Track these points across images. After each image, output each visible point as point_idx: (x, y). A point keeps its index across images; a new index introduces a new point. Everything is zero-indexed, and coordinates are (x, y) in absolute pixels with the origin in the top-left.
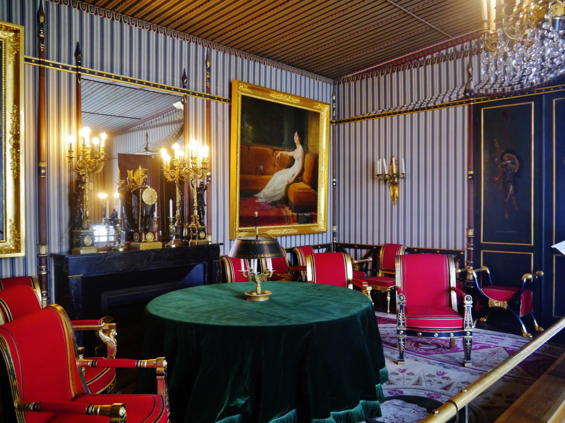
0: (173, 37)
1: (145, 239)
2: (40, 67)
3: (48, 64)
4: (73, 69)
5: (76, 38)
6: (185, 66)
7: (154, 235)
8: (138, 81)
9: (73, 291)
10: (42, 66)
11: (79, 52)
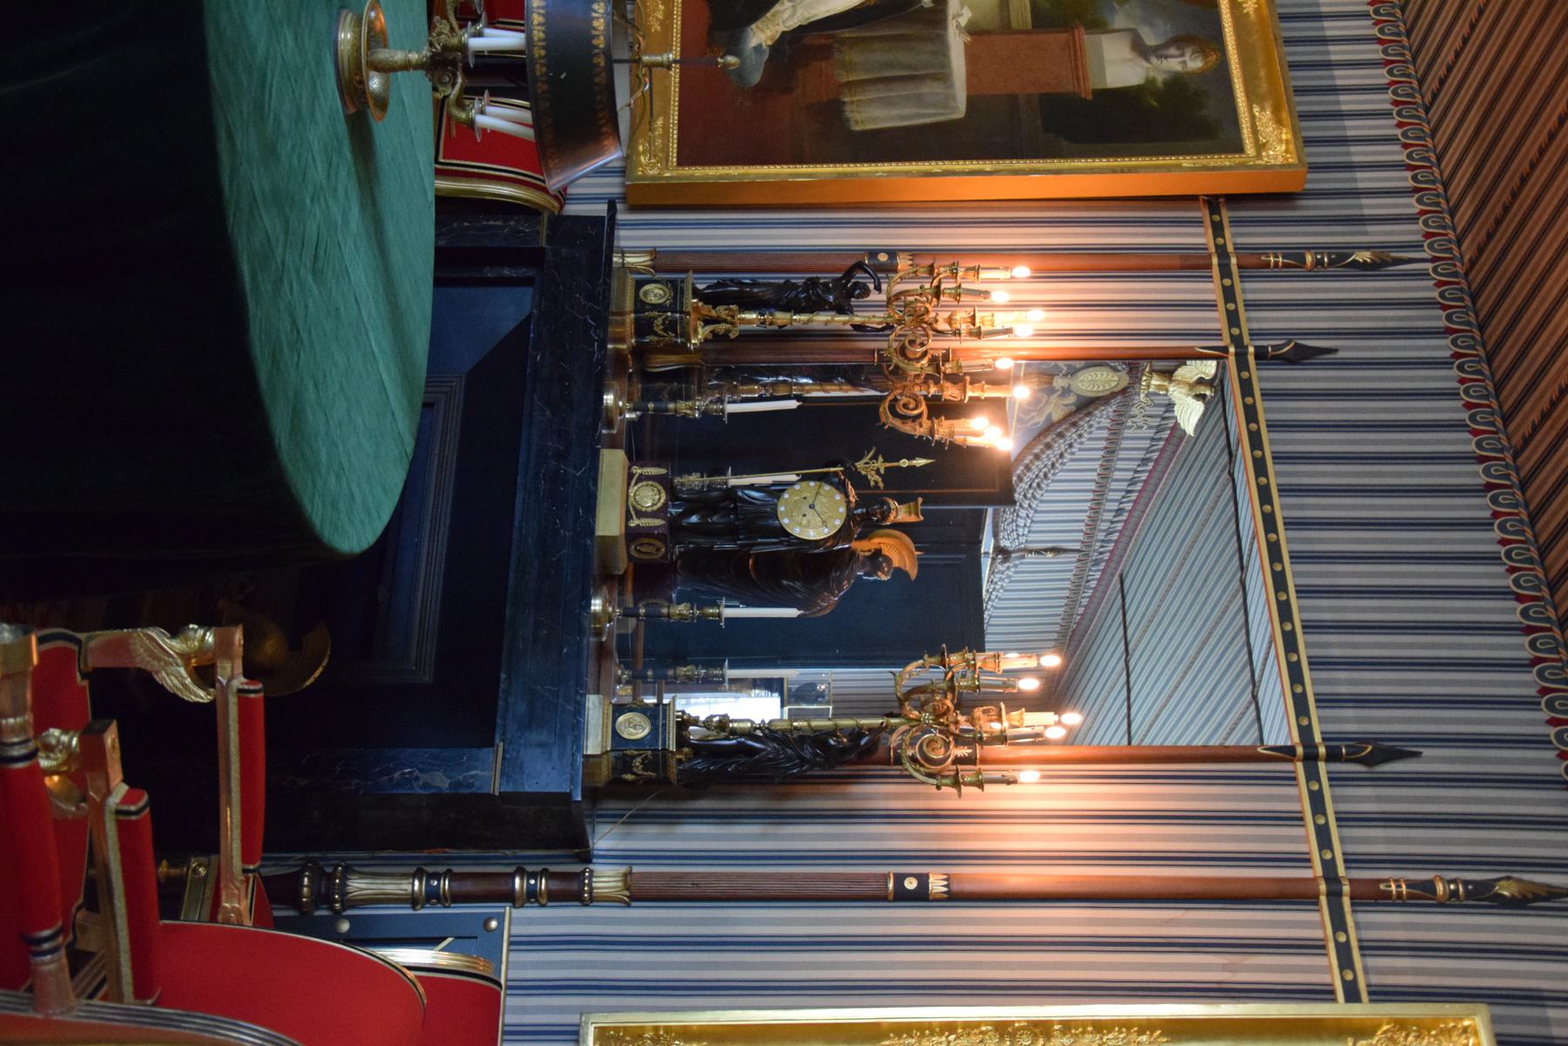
0: (1543, 701)
1: (641, 478)
2: (1210, 256)
3: (1225, 271)
4: (1237, 340)
5: (1349, 349)
6: (1433, 760)
7: (654, 515)
9: (499, 223)
10: (1215, 260)
11: (1300, 356)
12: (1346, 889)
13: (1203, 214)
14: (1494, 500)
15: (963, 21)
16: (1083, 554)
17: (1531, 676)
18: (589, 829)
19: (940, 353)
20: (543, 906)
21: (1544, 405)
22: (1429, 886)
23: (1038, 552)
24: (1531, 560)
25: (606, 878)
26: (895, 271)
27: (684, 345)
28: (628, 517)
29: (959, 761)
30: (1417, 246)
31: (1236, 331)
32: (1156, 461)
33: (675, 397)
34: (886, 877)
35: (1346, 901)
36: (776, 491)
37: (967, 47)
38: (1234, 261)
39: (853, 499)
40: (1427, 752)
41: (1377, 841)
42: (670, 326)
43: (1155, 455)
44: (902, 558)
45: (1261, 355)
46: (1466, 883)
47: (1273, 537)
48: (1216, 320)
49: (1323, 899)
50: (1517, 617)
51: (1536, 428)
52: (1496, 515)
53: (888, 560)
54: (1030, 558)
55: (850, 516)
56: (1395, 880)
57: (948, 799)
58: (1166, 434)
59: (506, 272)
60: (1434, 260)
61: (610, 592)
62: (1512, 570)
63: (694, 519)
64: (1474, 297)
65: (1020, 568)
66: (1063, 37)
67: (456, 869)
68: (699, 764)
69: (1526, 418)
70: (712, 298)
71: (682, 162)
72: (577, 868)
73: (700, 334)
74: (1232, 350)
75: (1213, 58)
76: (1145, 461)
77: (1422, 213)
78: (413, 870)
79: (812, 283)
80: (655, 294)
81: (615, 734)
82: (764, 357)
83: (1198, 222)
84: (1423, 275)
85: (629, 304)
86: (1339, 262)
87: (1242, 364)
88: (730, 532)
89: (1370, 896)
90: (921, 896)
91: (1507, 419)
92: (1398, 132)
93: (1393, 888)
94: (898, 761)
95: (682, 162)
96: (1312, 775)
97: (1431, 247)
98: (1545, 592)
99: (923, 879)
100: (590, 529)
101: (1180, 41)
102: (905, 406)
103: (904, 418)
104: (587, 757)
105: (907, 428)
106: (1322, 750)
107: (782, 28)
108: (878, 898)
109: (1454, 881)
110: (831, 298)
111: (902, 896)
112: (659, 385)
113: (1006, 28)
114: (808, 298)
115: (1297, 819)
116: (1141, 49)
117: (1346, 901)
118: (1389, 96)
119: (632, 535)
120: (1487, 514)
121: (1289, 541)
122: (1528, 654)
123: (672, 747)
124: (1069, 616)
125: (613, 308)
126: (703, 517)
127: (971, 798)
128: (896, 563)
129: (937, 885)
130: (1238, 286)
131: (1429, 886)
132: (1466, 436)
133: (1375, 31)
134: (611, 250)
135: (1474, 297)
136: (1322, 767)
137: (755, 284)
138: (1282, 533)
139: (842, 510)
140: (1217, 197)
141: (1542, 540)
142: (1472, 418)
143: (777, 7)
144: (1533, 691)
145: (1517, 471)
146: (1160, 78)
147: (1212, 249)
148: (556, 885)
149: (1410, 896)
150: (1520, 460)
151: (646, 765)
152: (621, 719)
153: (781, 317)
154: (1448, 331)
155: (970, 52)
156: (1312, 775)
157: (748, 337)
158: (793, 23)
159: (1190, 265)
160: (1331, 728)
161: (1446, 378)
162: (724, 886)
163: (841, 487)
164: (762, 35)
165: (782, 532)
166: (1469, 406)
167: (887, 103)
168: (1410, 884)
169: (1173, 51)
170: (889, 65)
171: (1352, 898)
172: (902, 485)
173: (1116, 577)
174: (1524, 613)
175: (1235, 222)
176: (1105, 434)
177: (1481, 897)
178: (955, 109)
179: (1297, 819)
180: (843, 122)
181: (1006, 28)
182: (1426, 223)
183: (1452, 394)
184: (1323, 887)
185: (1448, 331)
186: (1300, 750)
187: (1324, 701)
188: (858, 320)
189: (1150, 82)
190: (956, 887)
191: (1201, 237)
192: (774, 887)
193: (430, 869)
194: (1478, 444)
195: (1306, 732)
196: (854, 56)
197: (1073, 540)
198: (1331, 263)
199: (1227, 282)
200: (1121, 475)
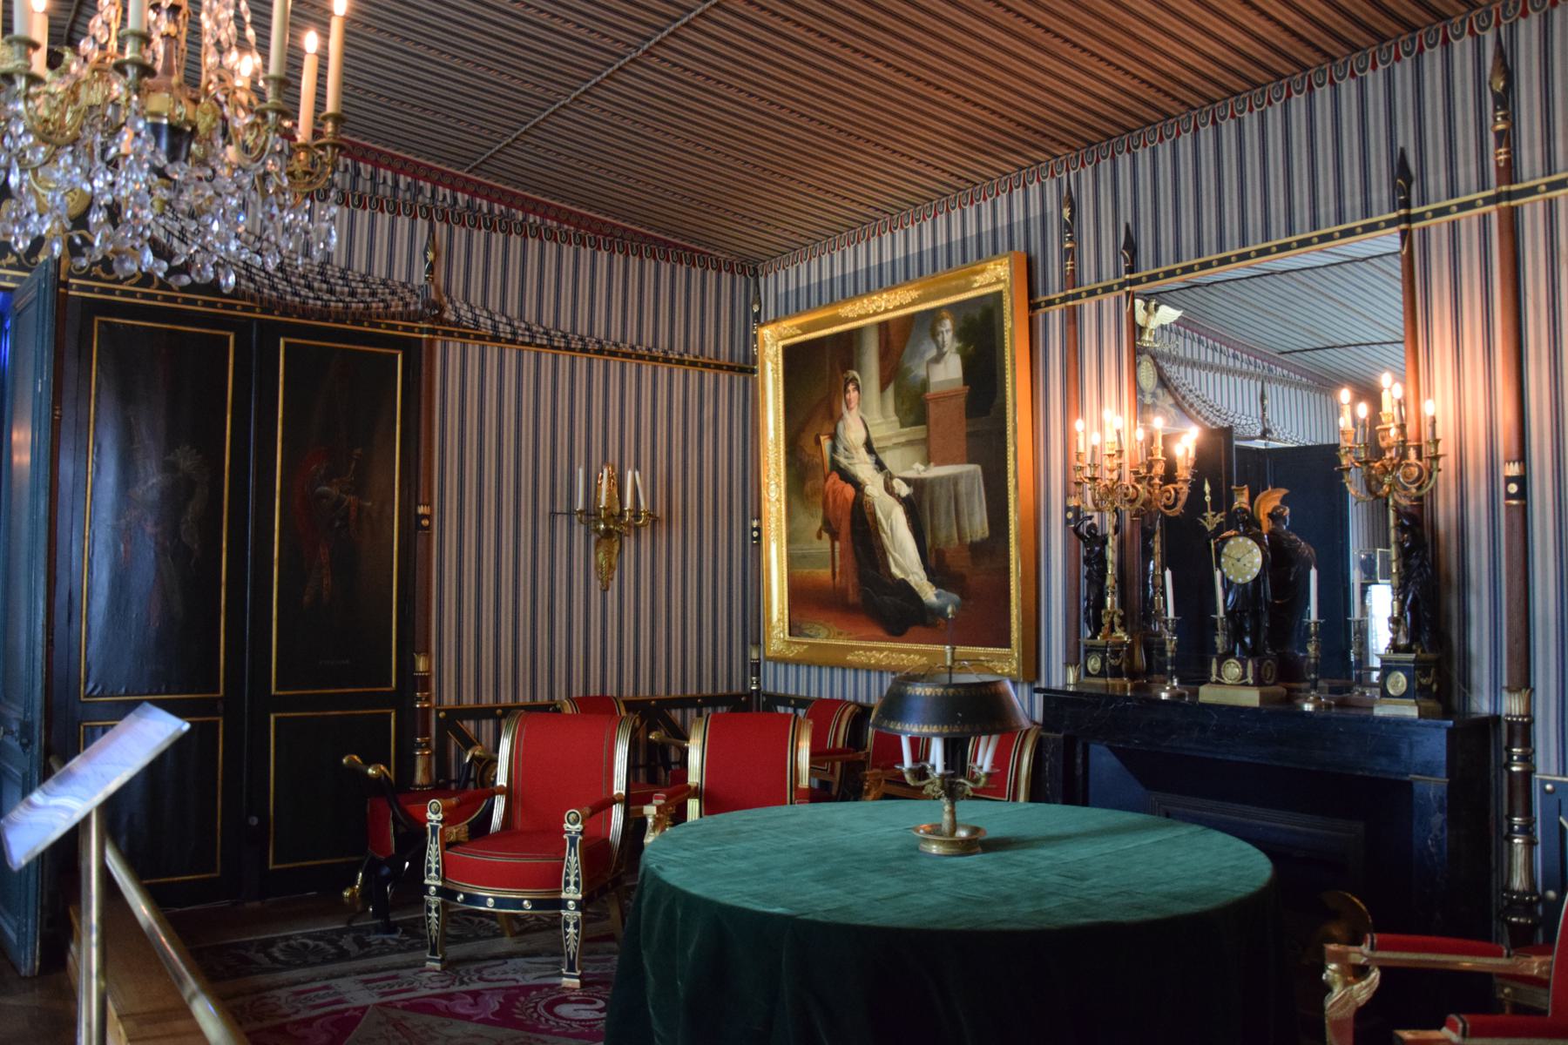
0: (1359, 75)
1: (1219, 675)
2: (1068, 307)
3: (1077, 296)
4: (1121, 286)
5: (1126, 216)
6: (1406, 138)
8: (1200, 264)
10: (1070, 303)
11: (1131, 246)
12: (1504, 188)
13: (1040, 313)
14: (1223, 118)
15: (922, 468)
16: (1265, 379)
17: (1343, 84)
18: (1474, 716)
19: (1133, 476)
20: (1534, 751)
21: (1160, 96)
22: (1500, 135)
23: (1264, 410)
24: (1263, 93)
25: (1512, 706)
26: (1078, 507)
27: (1128, 645)
28: (1246, 684)
29: (1419, 457)
30: (1059, 181)
31: (1116, 287)
32: (1200, 334)
33: (1163, 651)
34: (1508, 506)
35: (1514, 187)
36: (1228, 585)
37: (938, 464)
38: (1070, 292)
39: (1233, 533)
40: (1400, 143)
41: (1467, 170)
42: (1116, 654)
43: (1196, 335)
44: (1274, 499)
45: (1131, 270)
46: (1495, 110)
47: (1253, 254)
48: (1109, 300)
49: (1513, 203)
50: (1302, 97)
51: (1175, 99)
52: (1233, 116)
53: (1275, 509)
54: (1268, 415)
55: (1245, 534)
56: (1497, 156)
57: (1448, 464)
58: (1182, 329)
59: (1079, 761)
60: (1068, 171)
61: (1298, 698)
62: (1270, 103)
63: (1247, 640)
64: (1091, 144)
65: (1275, 421)
66: (931, 405)
67: (1506, 812)
68: (1425, 637)
69: (1170, 107)
70: (1097, 627)
71: (1008, 645)
72: (1505, 727)
73: (1120, 633)
74: (1128, 289)
75: (944, 313)
76: (1200, 342)
77: (1039, 180)
78: (1506, 844)
79: (1087, 561)
80: (1094, 664)
81: (1403, 696)
82: (1136, 592)
83: (1046, 315)
84: (1078, 176)
85: (1101, 681)
86: (1070, 227)
87: (1138, 281)
88: (1256, 615)
89: (1510, 171)
90: (1522, 481)
91: (1169, 116)
92: (989, 200)
93: (1502, 157)
94: (1420, 499)
95: (1008, 645)
96: (1421, 217)
97: (1059, 173)
98: (1285, 81)
99: (1509, 480)
100: (1254, 709)
101: (934, 334)
102: (1168, 499)
103: (1176, 499)
104: (1420, 716)
105: (1183, 497)
106: (1402, 212)
107: (925, 581)
108: (1525, 511)
109: (1495, 120)
110: (1097, 548)
111: (1523, 494)
112: (1155, 664)
113: (925, 441)
114: (1097, 564)
115: (1454, 226)
116: (938, 359)
117: (1514, 187)
118: (967, 207)
119: (1259, 682)
120: (1233, 122)
121: (1255, 244)
122: (1327, 87)
123: (1412, 656)
124: (1308, 387)
125: (1104, 692)
126: (1247, 634)
127: (1447, 448)
128: (1277, 503)
129: (1513, 470)
130: (1086, 288)
131: (1500, 135)
132: (1181, 139)
133: (929, 220)
134: (1065, 692)
135: (1091, 144)
136: (1414, 211)
137: (1088, 599)
138: (1250, 248)
139: (1241, 539)
140: (1030, 305)
141: (1248, 87)
142: (1169, 137)
143: (913, 584)
144: (1353, 82)
145: (1203, 106)
146: (957, 345)
147: (1063, 305)
148: (1518, 741)
149: (1508, 145)
150: (1195, 105)
151: (1426, 674)
152: (1391, 692)
153: (1110, 581)
154: (1113, 157)
155: (943, 462)
156: (1421, 217)
157: (1123, 602)
158: (923, 574)
159: (1073, 319)
160: (1386, 206)
161: (1144, 155)
162: (1517, 621)
163: (1225, 541)
164: (929, 594)
165: (1256, 580)
166: (1161, 140)
167: (971, 515)
168: (1499, 146)
169: (940, 339)
170: (948, 513)
171: (1511, 183)
172: (1223, 500)
173: (1282, 357)
174: (1299, 92)
175: (1045, 292)
176: (1182, 369)
177: (1506, 100)
178: (975, 471)
179: (1454, 226)
180: (983, 542)
181: (925, 441)
182: (1045, 178)
183: (1154, 151)
184: (1504, 204)
185: (1113, 157)
186: (1403, 226)
187: (1367, 213)
188: (1111, 531)
189: (959, 351)
190: (1515, 456)
191: (1055, 313)
192: (1518, 584)
193: (1505, 831)
194: (1186, 131)
195: (1390, 223)
196: (942, 535)
197: (1254, 387)
198: (1071, 232)
199: (1084, 295)
200: (1209, 357)
